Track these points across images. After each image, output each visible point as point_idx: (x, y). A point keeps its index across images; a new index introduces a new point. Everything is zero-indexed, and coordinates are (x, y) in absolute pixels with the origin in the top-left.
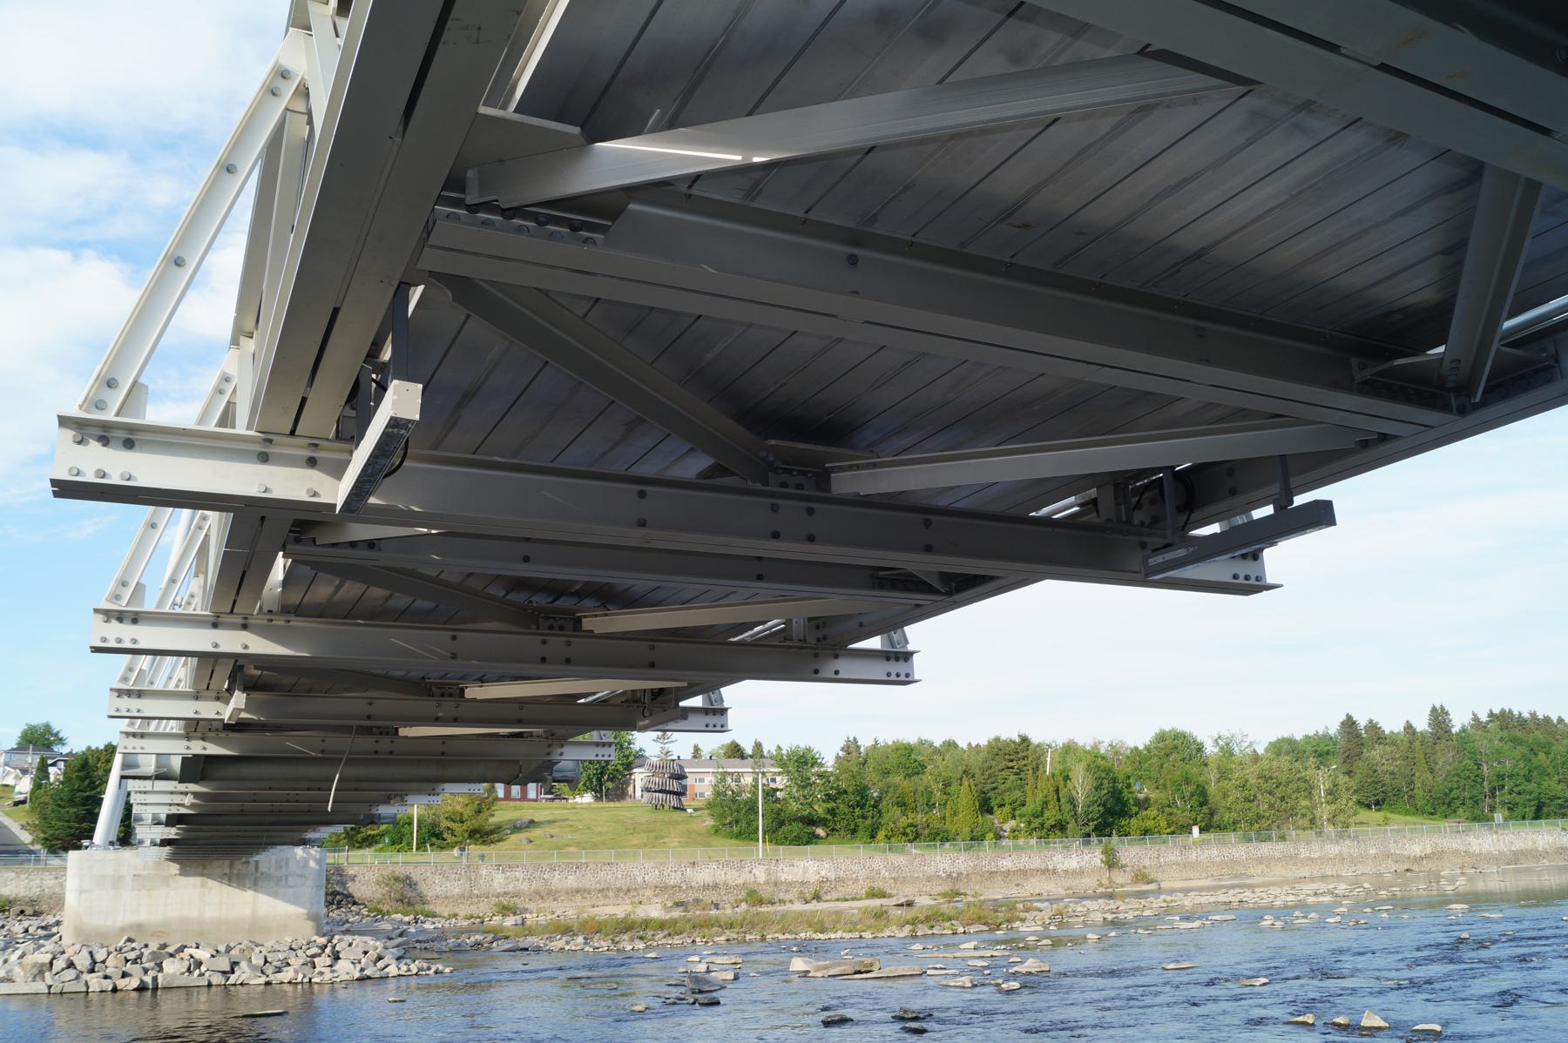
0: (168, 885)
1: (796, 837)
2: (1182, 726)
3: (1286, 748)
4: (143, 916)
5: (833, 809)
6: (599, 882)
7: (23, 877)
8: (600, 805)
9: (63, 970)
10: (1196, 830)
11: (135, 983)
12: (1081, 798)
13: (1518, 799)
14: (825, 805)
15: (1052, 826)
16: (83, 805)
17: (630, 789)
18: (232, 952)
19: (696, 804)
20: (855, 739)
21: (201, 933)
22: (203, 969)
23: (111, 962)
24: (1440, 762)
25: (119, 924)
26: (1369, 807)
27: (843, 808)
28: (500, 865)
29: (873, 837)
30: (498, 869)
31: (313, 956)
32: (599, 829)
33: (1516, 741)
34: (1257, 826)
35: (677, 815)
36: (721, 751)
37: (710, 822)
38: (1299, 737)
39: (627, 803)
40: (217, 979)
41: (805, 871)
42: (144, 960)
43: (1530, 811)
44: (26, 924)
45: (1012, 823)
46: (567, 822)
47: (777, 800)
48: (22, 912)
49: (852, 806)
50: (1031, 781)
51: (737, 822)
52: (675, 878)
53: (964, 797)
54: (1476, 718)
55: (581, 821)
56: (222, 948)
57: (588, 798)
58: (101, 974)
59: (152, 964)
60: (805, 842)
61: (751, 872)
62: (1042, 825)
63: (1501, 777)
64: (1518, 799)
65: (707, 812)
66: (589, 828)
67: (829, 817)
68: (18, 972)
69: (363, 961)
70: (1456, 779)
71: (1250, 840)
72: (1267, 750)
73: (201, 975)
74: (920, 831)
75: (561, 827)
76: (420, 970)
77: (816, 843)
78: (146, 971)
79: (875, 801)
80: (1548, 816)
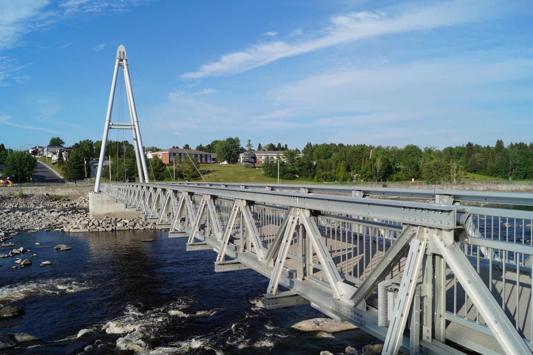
3: (450, 151)
4: (110, 211)
5: (301, 169)
7: (64, 190)
8: (229, 165)
10: (413, 179)
11: (111, 229)
13: (520, 172)
14: (298, 168)
16: (78, 169)
17: (239, 160)
18: (134, 221)
20: (310, 143)
21: (125, 215)
22: (127, 225)
23: (104, 223)
24: (497, 159)
25: (104, 213)
26: (472, 172)
29: (313, 178)
32: (230, 174)
33: (522, 153)
35: (253, 169)
37: (263, 172)
38: (454, 147)
39: (238, 164)
40: (131, 228)
42: (112, 223)
43: (522, 176)
44: (67, 204)
45: (357, 175)
47: (284, 166)
48: (64, 200)
49: (307, 169)
50: (363, 162)
51: (272, 172)
53: (342, 166)
56: (132, 220)
57: (225, 162)
58: (101, 227)
59: (114, 224)
62: (366, 176)
63: (515, 165)
64: (520, 172)
66: (226, 173)
67: (300, 172)
70: (500, 165)
71: (429, 184)
73: (127, 227)
74: (328, 177)
77: (296, 179)
78: (113, 226)
79: (314, 167)
80: (529, 178)
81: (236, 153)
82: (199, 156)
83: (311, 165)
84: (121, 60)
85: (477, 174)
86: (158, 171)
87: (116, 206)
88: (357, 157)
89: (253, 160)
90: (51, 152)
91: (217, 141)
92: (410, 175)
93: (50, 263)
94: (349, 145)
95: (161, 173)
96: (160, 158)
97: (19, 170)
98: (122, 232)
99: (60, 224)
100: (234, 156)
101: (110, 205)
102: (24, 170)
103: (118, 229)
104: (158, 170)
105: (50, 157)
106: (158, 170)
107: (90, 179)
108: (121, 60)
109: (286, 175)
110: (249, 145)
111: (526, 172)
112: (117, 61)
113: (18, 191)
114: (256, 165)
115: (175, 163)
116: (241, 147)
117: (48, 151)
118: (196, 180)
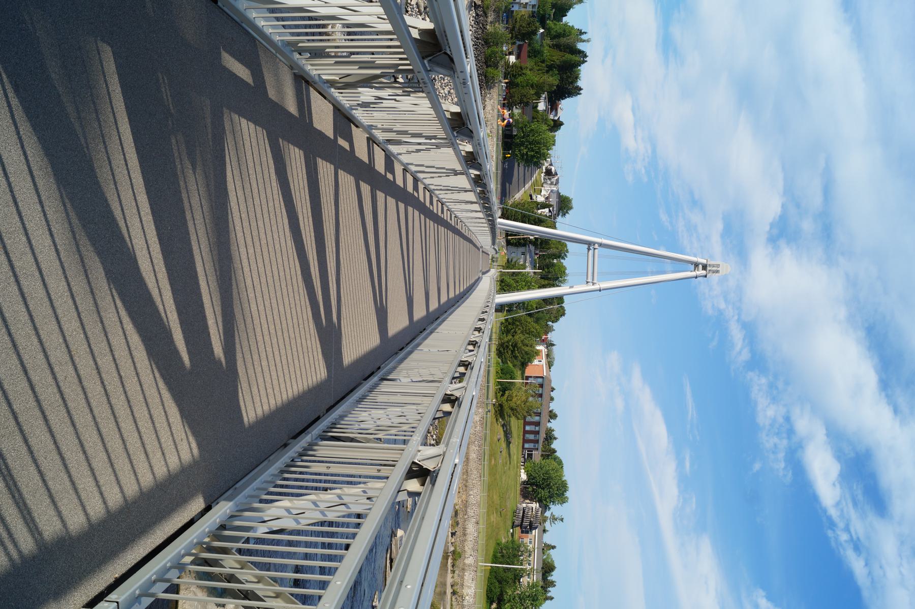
1: (492, 590)
6: (471, 470)
17: (528, 501)
28: (483, 419)
30: (481, 418)
32: (504, 479)
35: (510, 523)
36: (550, 560)
37: (504, 541)
39: (519, 498)
41: (469, 587)
46: (508, 463)
47: (515, 582)
52: (471, 512)
55: (509, 468)
57: (524, 477)
60: (488, 595)
61: (471, 555)
66: (504, 472)
75: (506, 457)
77: (487, 602)
81: (539, 496)
82: (537, 428)
84: (705, 267)
89: (526, 523)
90: (549, 194)
95: (510, 352)
96: (536, 362)
97: (522, 141)
100: (535, 493)
102: (522, 148)
104: (516, 349)
105: (542, 194)
107: (505, 245)
108: (705, 267)
109: (497, 584)
110: (554, 519)
112: (704, 261)
113: (491, 132)
114: (518, 529)
115: (527, 383)
116: (551, 506)
117: (552, 191)
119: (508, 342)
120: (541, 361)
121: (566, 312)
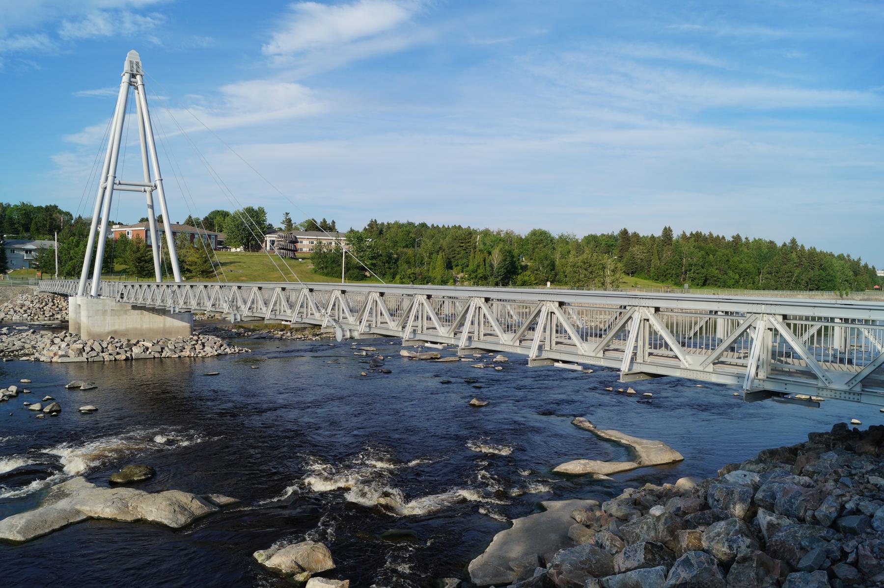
0: (126, 314)
2: (544, 228)
3: (592, 240)
4: (116, 327)
9: (90, 351)
10: (549, 283)
11: (124, 357)
12: (495, 264)
14: (371, 261)
15: (481, 277)
19: (303, 255)
20: (375, 220)
21: (142, 335)
22: (150, 350)
23: (110, 347)
24: (664, 255)
26: (628, 274)
27: (380, 263)
29: (394, 278)
31: (194, 345)
32: (255, 268)
34: (577, 284)
35: (293, 261)
37: (311, 267)
38: (599, 234)
40: (157, 355)
42: (124, 347)
43: (700, 282)
45: (461, 275)
46: (239, 264)
51: (326, 267)
53: (440, 260)
54: (684, 234)
55: (244, 263)
56: (156, 342)
62: (476, 276)
63: (691, 265)
65: (310, 261)
66: (249, 267)
68: (71, 353)
69: (215, 347)
72: (583, 240)
74: (417, 276)
76: (239, 350)
77: (366, 280)
83: (389, 256)
84: (133, 76)
85: (636, 277)
86: (143, 261)
87: (126, 319)
88: (460, 247)
89: (291, 246)
91: (218, 211)
92: (542, 276)
93: (95, 408)
94: (435, 226)
95: (147, 265)
98: (141, 362)
99: (21, 350)
101: (116, 317)
103: (136, 358)
104: (143, 258)
106: (143, 258)
108: (133, 76)
111: (706, 276)
116: (268, 223)
118: (207, 277)
119: (137, 267)
120: (128, 232)
121: (53, 204)
